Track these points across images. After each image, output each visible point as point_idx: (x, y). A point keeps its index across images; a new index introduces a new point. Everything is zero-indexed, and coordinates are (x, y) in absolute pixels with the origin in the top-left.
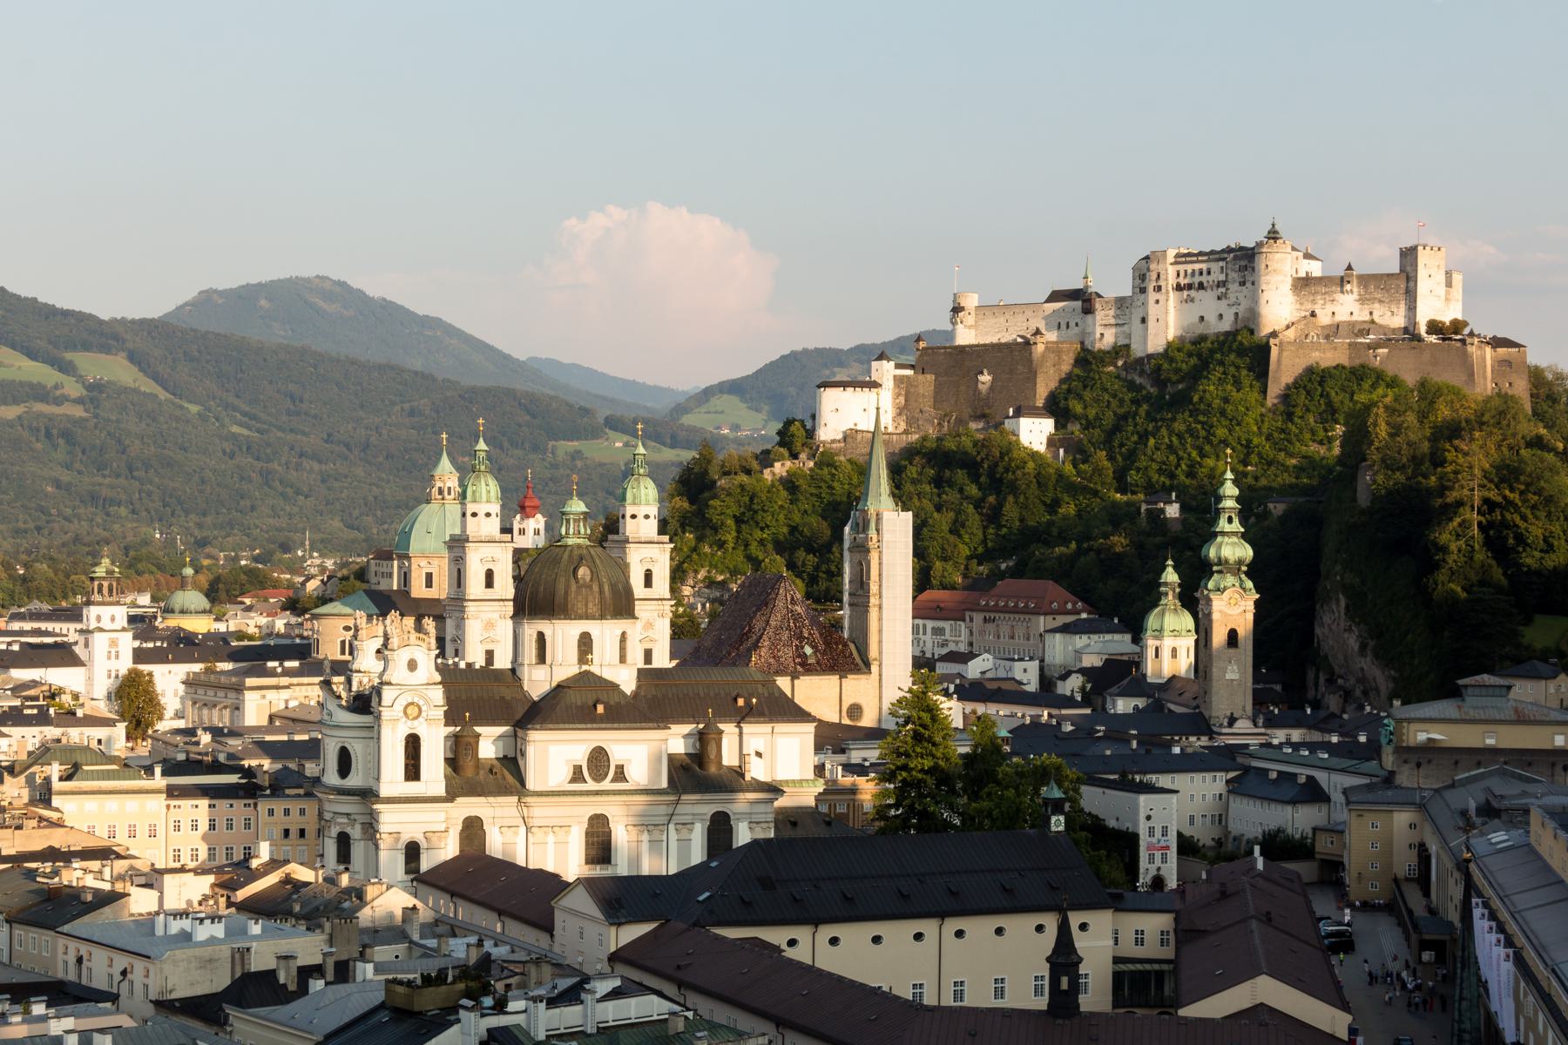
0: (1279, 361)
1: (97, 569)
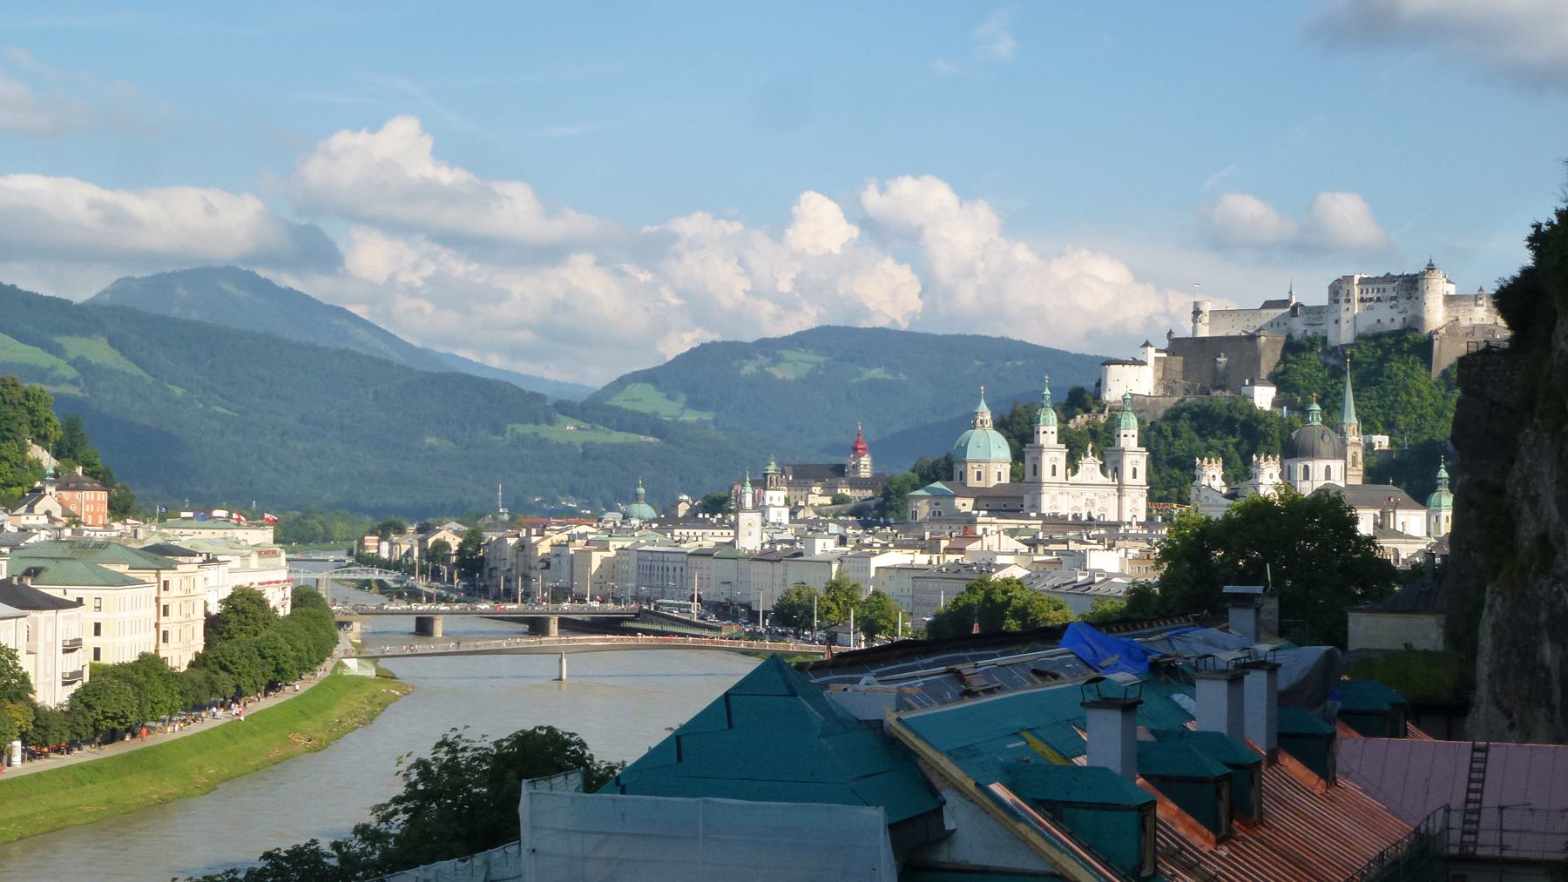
0: (1440, 349)
1: (769, 468)
